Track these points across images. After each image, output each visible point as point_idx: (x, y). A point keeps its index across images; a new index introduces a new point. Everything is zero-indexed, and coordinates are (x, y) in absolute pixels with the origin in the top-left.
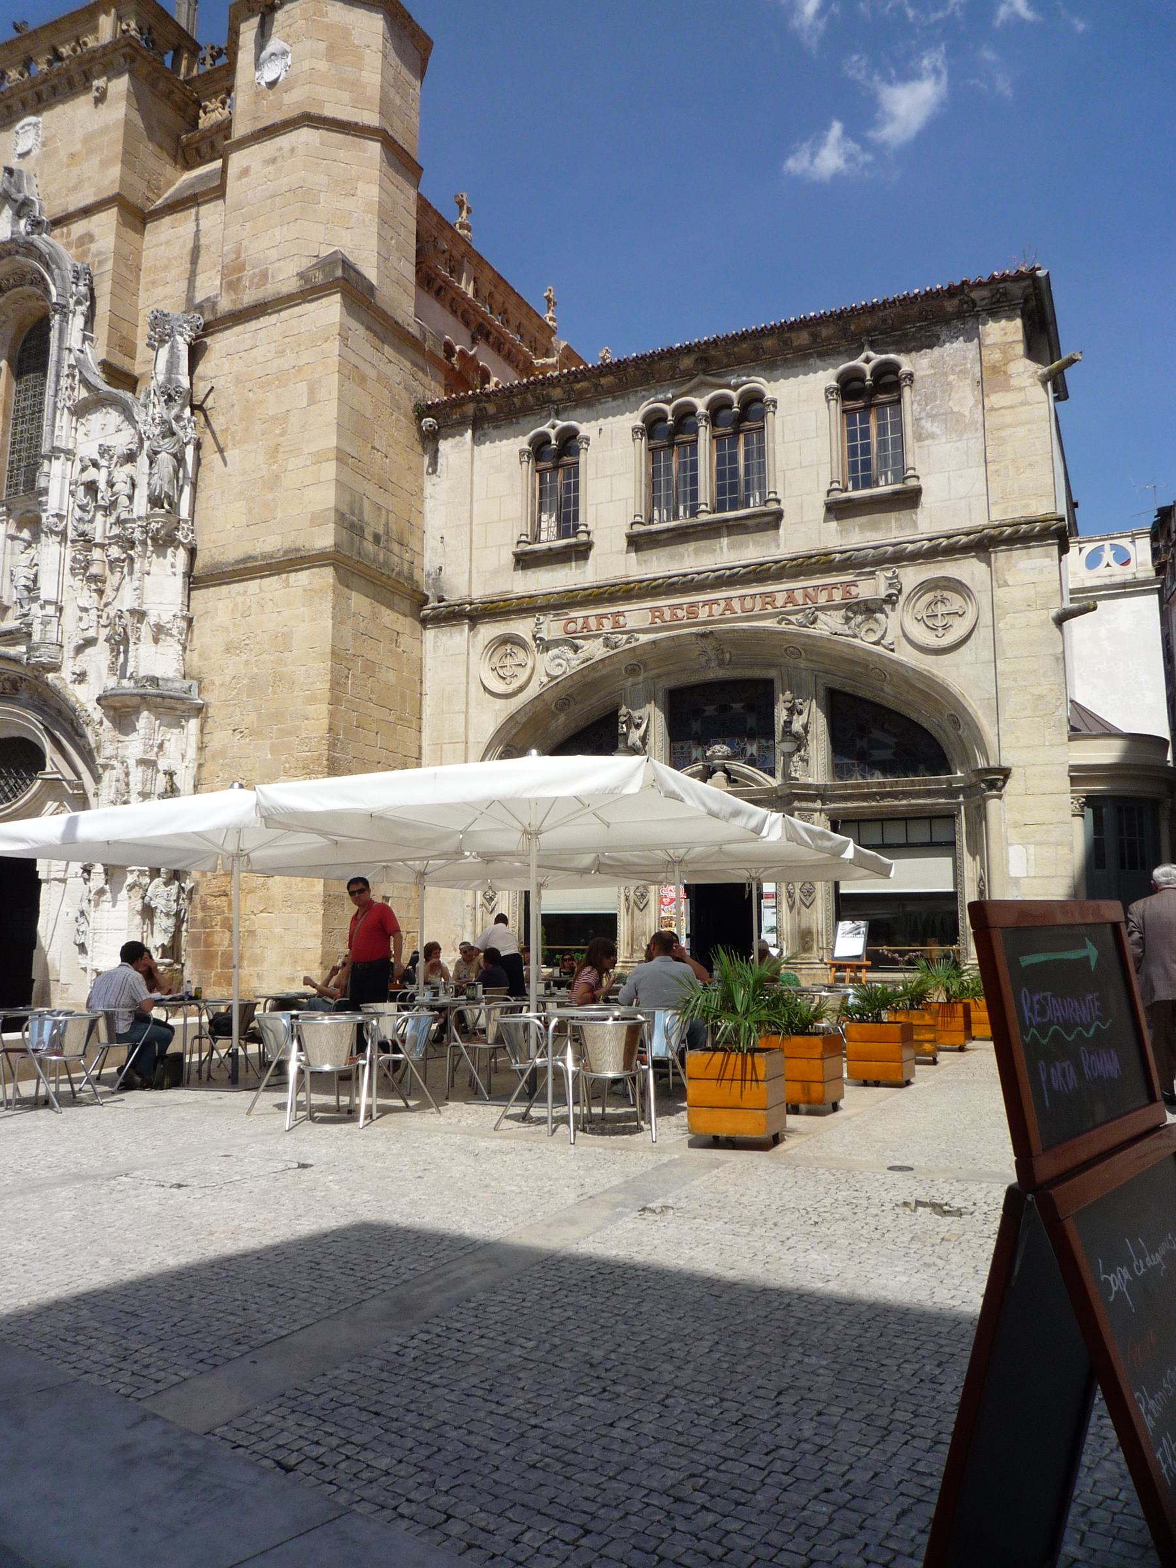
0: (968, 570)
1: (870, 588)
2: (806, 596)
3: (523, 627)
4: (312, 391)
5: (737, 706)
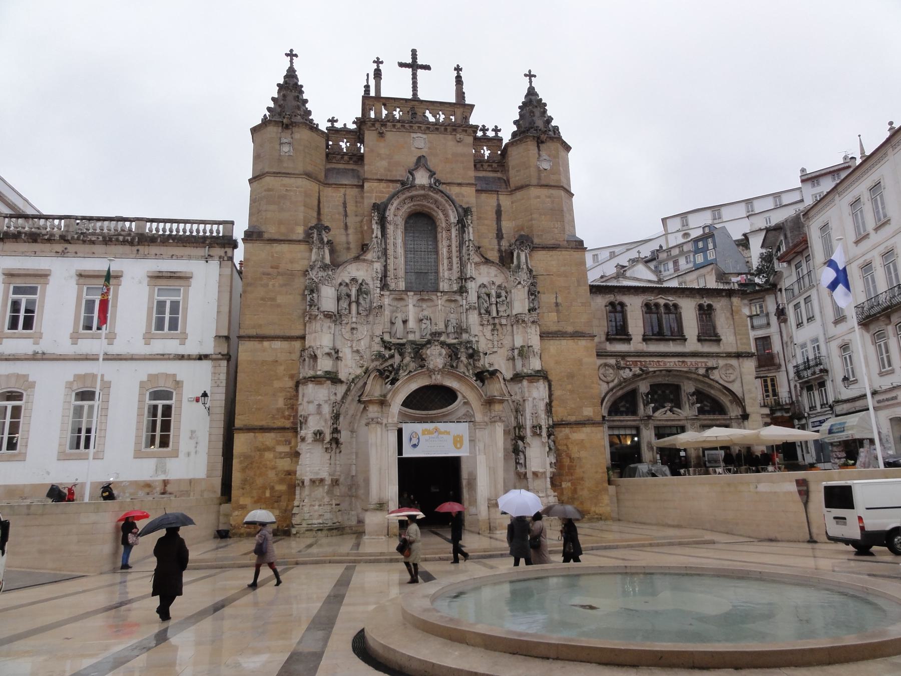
0: (734, 362)
1: (711, 362)
2: (696, 364)
3: (612, 361)
4: (578, 281)
5: (667, 392)
